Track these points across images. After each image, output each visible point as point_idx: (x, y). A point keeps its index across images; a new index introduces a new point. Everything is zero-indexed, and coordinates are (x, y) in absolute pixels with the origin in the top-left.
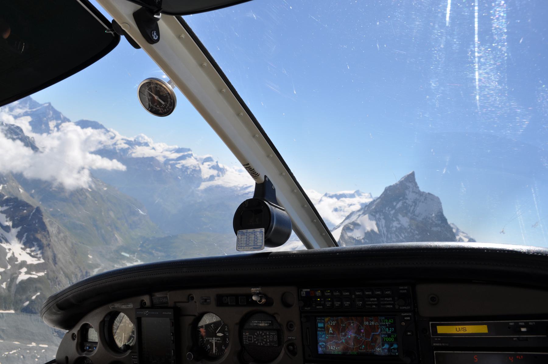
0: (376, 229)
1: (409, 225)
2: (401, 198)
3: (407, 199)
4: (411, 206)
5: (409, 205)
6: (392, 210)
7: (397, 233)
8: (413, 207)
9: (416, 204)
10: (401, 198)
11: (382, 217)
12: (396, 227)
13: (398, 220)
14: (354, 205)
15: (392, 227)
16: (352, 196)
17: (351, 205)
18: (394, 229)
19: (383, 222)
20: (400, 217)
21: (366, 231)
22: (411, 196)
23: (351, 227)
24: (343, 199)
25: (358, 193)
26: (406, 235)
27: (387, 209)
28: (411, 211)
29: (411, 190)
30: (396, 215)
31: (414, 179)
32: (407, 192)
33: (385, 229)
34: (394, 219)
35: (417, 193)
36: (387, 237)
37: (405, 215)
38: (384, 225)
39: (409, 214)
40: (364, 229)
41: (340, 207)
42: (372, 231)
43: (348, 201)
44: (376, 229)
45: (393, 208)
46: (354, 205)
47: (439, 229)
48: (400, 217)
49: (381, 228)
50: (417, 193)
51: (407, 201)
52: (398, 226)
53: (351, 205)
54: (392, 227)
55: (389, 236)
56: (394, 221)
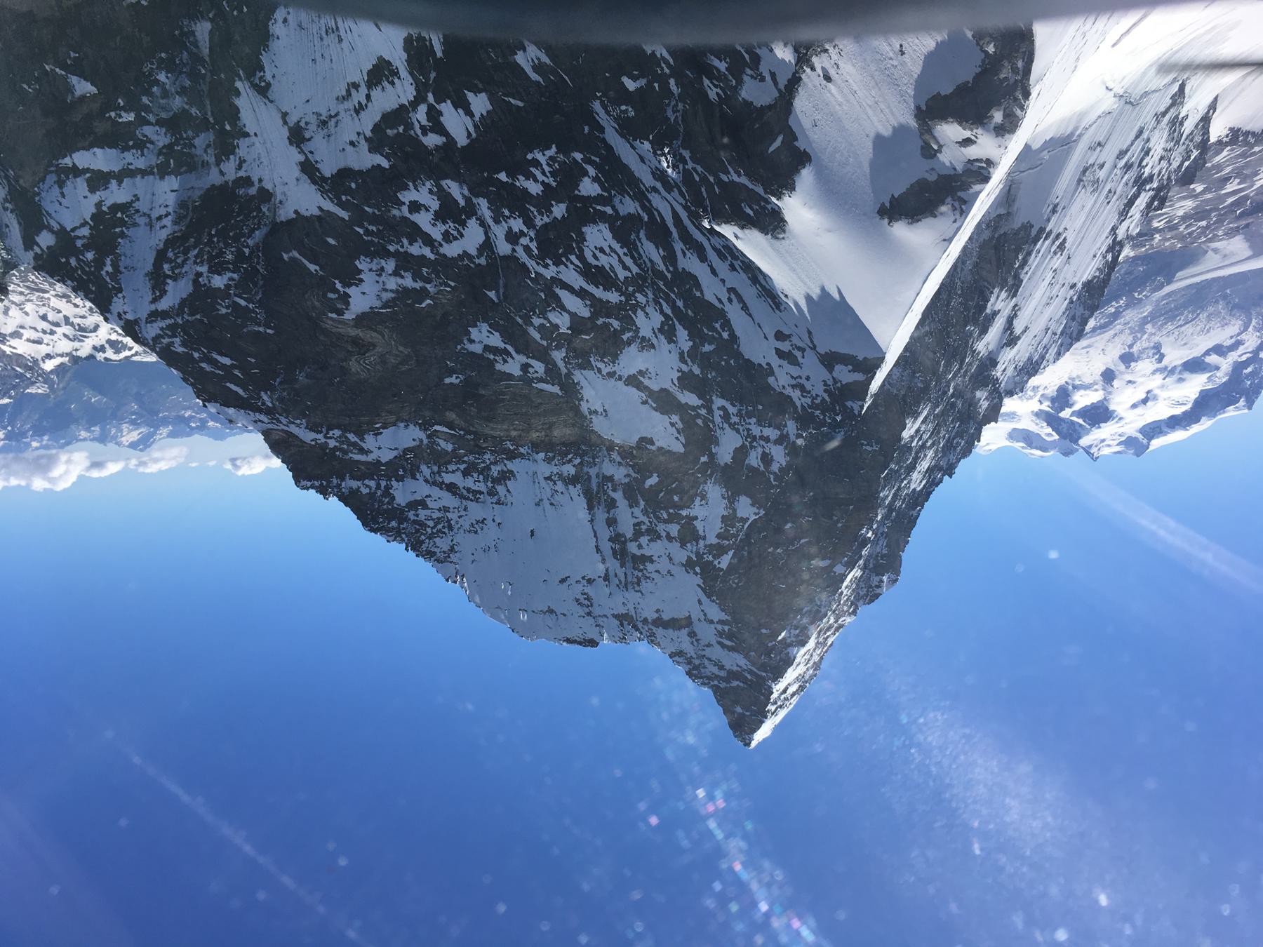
0: (751, 244)
1: (571, 391)
2: (725, 562)
3: (689, 565)
4: (638, 534)
5: (654, 535)
6: (741, 453)
7: (613, 297)
8: (627, 529)
9: (621, 554)
10: (725, 562)
11: (782, 378)
12: (647, 345)
13: (664, 402)
14: (1134, 406)
15: (668, 332)
16: (1153, 430)
17: (1145, 401)
18: (648, 322)
19: (758, 349)
20: (664, 433)
21: (806, 177)
22: (676, 592)
23: (950, 131)
24: (1178, 411)
25: (1134, 445)
26: (562, 321)
27: (779, 456)
28: (618, 496)
29: (707, 633)
30: (700, 437)
31: (722, 696)
32: (715, 612)
33: (711, 290)
34: (690, 399)
35: (659, 622)
36: (659, 234)
37: (639, 455)
38: (734, 312)
39: (620, 473)
40: (835, 196)
41: (1181, 380)
42: (772, 223)
43: (1159, 411)
44: (751, 244)
45: (737, 478)
46: (1134, 406)
47: (385, 444)
48: (664, 433)
49: (740, 281)
50: (659, 622)
51: (681, 555)
52: (632, 360)
53: (1145, 401)
54: (668, 332)
55: (651, 251)
56: (686, 381)
